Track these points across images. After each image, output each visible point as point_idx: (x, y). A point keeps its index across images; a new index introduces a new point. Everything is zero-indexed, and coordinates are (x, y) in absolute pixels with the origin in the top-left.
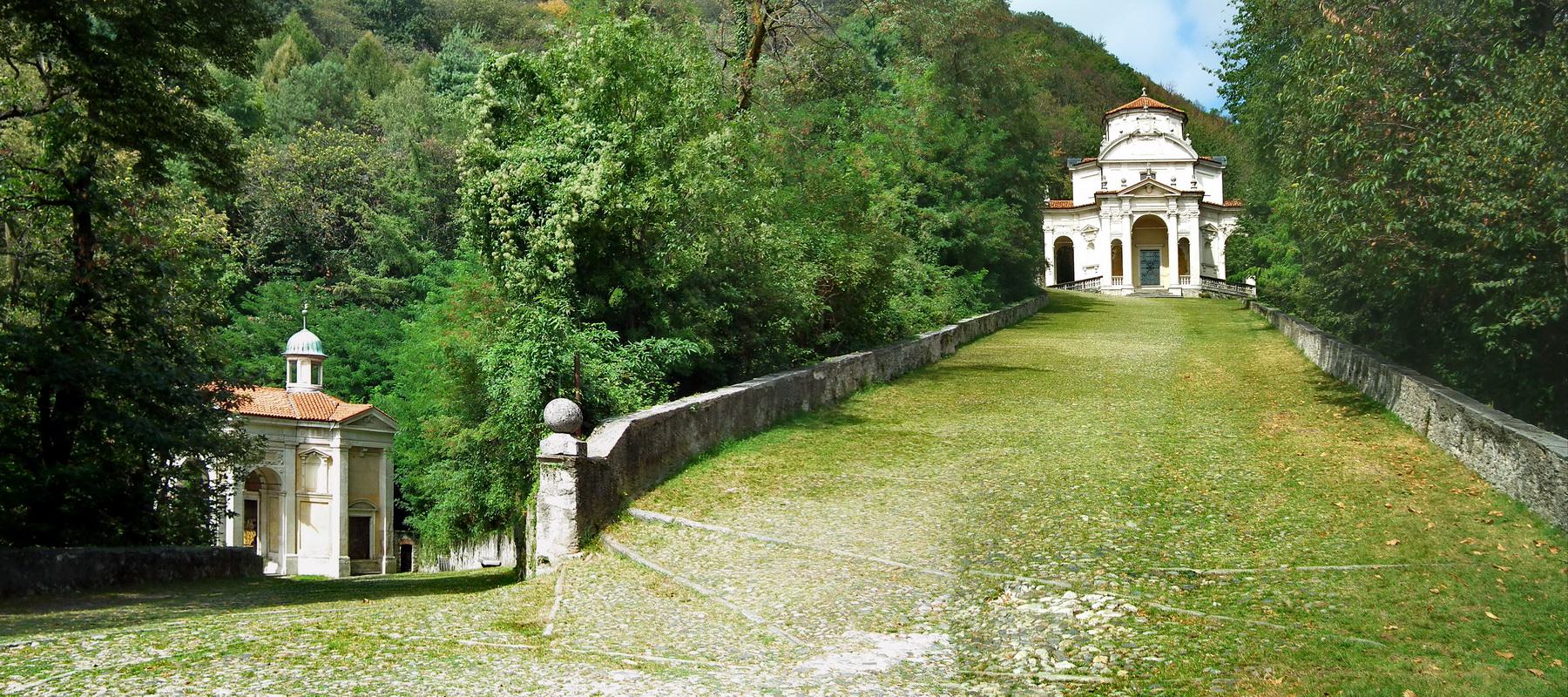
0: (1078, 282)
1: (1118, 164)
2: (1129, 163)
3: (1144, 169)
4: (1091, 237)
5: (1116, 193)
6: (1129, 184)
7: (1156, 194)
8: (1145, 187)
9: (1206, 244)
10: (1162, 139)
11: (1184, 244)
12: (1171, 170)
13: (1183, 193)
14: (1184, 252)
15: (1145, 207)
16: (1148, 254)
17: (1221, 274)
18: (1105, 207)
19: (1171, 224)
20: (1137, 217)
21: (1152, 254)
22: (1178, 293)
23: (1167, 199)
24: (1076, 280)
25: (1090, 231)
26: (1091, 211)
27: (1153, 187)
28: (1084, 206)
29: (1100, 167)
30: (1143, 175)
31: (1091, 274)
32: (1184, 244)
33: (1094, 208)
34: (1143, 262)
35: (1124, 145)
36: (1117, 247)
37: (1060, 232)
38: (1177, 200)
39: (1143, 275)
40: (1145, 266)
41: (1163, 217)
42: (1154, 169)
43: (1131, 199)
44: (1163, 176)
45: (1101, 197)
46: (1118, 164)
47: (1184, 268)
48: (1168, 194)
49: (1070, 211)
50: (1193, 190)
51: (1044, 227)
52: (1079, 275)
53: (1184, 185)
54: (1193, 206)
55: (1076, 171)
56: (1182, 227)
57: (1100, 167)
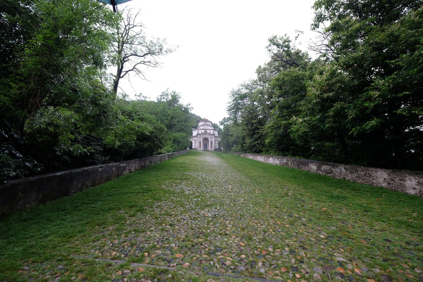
1: (201, 129)
7: (207, 134)
9: (215, 143)
11: (212, 142)
15: (205, 136)
18: (198, 136)
19: (209, 139)
25: (195, 140)
30: (205, 131)
32: (212, 142)
33: (196, 136)
36: (200, 142)
44: (208, 131)
45: (198, 134)
46: (201, 129)
48: (210, 134)
52: (193, 147)
53: (212, 133)
54: (213, 136)
56: (212, 140)
57: (198, 130)
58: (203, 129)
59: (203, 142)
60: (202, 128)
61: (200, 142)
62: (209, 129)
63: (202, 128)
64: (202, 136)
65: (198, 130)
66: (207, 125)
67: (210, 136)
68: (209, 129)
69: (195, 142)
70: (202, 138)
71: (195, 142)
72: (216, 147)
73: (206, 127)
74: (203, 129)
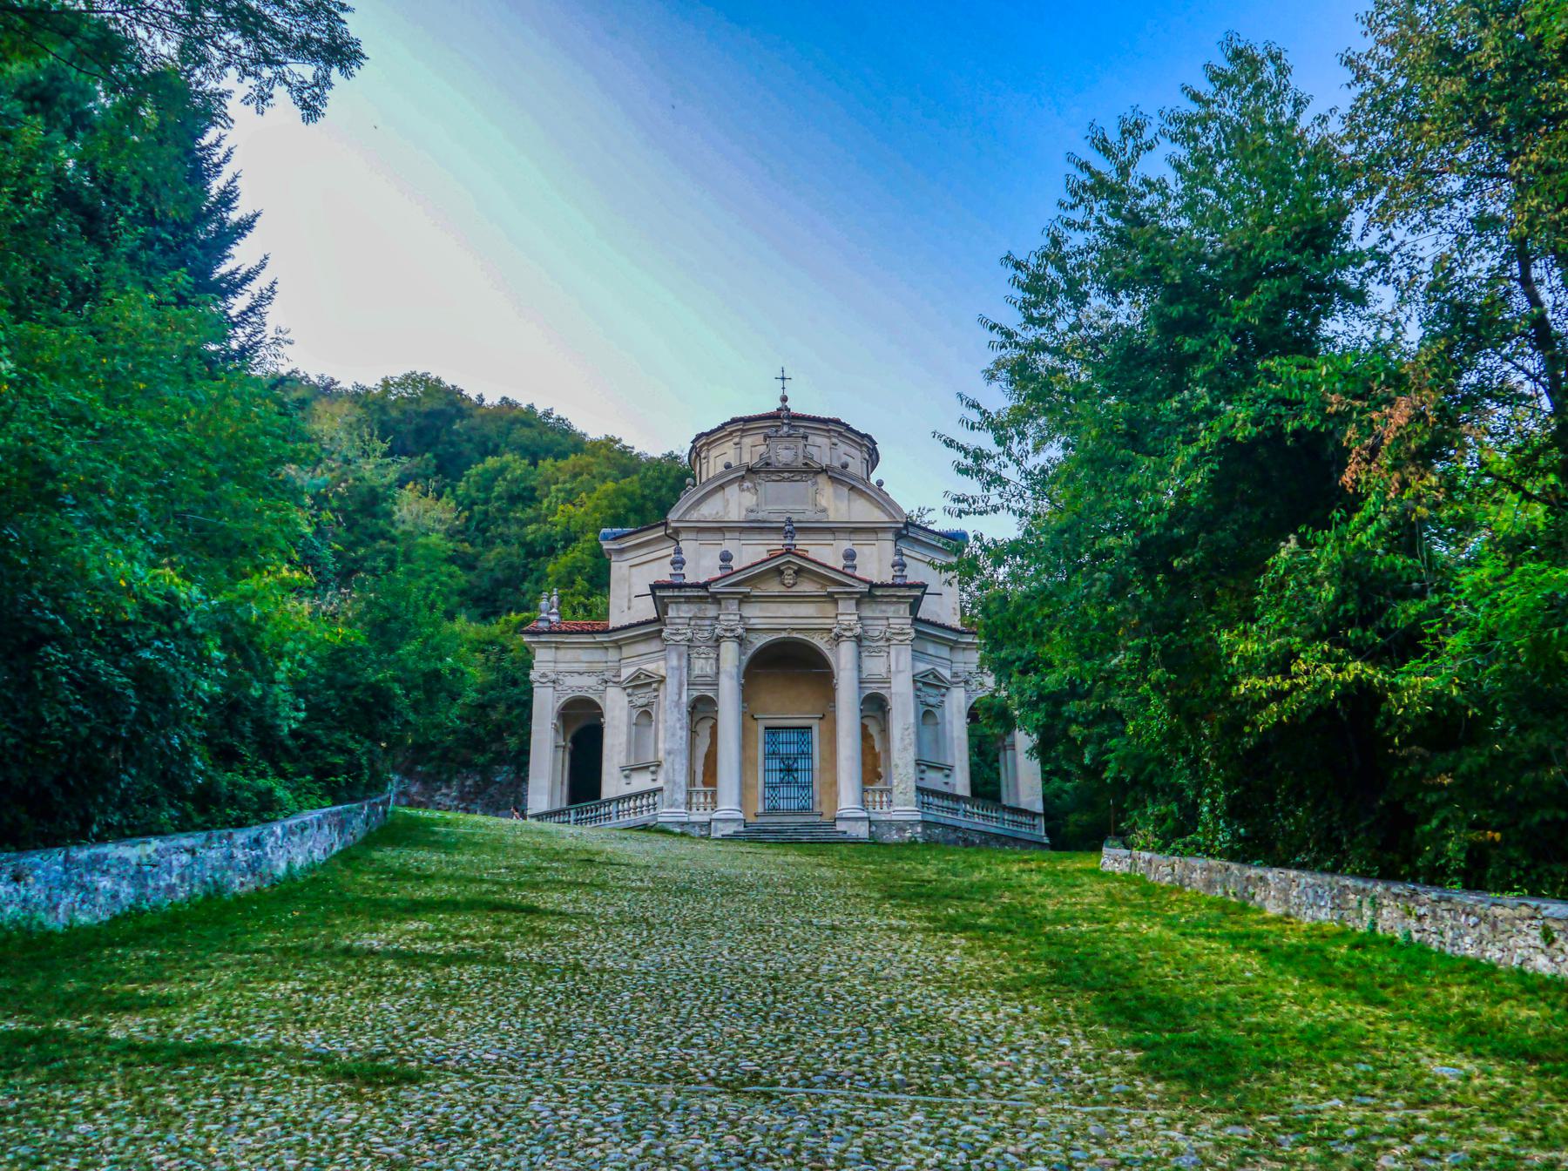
0: (610, 801)
1: (720, 529)
2: (742, 530)
3: (777, 543)
4: (641, 698)
5: (705, 586)
6: (736, 565)
7: (806, 587)
8: (778, 571)
9: (928, 715)
10: (822, 479)
11: (875, 706)
12: (845, 545)
13: (873, 586)
14: (874, 730)
16: (782, 737)
17: (961, 783)
18: (679, 613)
19: (843, 660)
20: (759, 641)
21: (794, 737)
22: (862, 831)
23: (832, 598)
24: (604, 797)
25: (642, 682)
26: (647, 637)
27: (800, 572)
28: (631, 626)
29: (674, 536)
31: (642, 782)
32: (875, 706)
34: (770, 755)
35: (733, 490)
36: (702, 709)
37: (580, 685)
38: (858, 603)
39: (772, 787)
40: (776, 764)
41: (819, 642)
42: (801, 543)
43: (745, 599)
47: (873, 769)
49: (599, 638)
50: (898, 581)
51: (533, 675)
52: (612, 785)
54: (898, 616)
55: (622, 551)
57: (674, 536)
58: (753, 528)
59: (748, 716)
60: (735, 504)
61: (702, 709)
62: (833, 530)
63: (735, 504)
64: (730, 615)
65: (688, 546)
66: (810, 471)
67: (847, 614)
68: (833, 530)
69: (645, 714)
70: (729, 651)
71: (645, 714)
72: (934, 780)
73: (780, 501)
74: (753, 528)
